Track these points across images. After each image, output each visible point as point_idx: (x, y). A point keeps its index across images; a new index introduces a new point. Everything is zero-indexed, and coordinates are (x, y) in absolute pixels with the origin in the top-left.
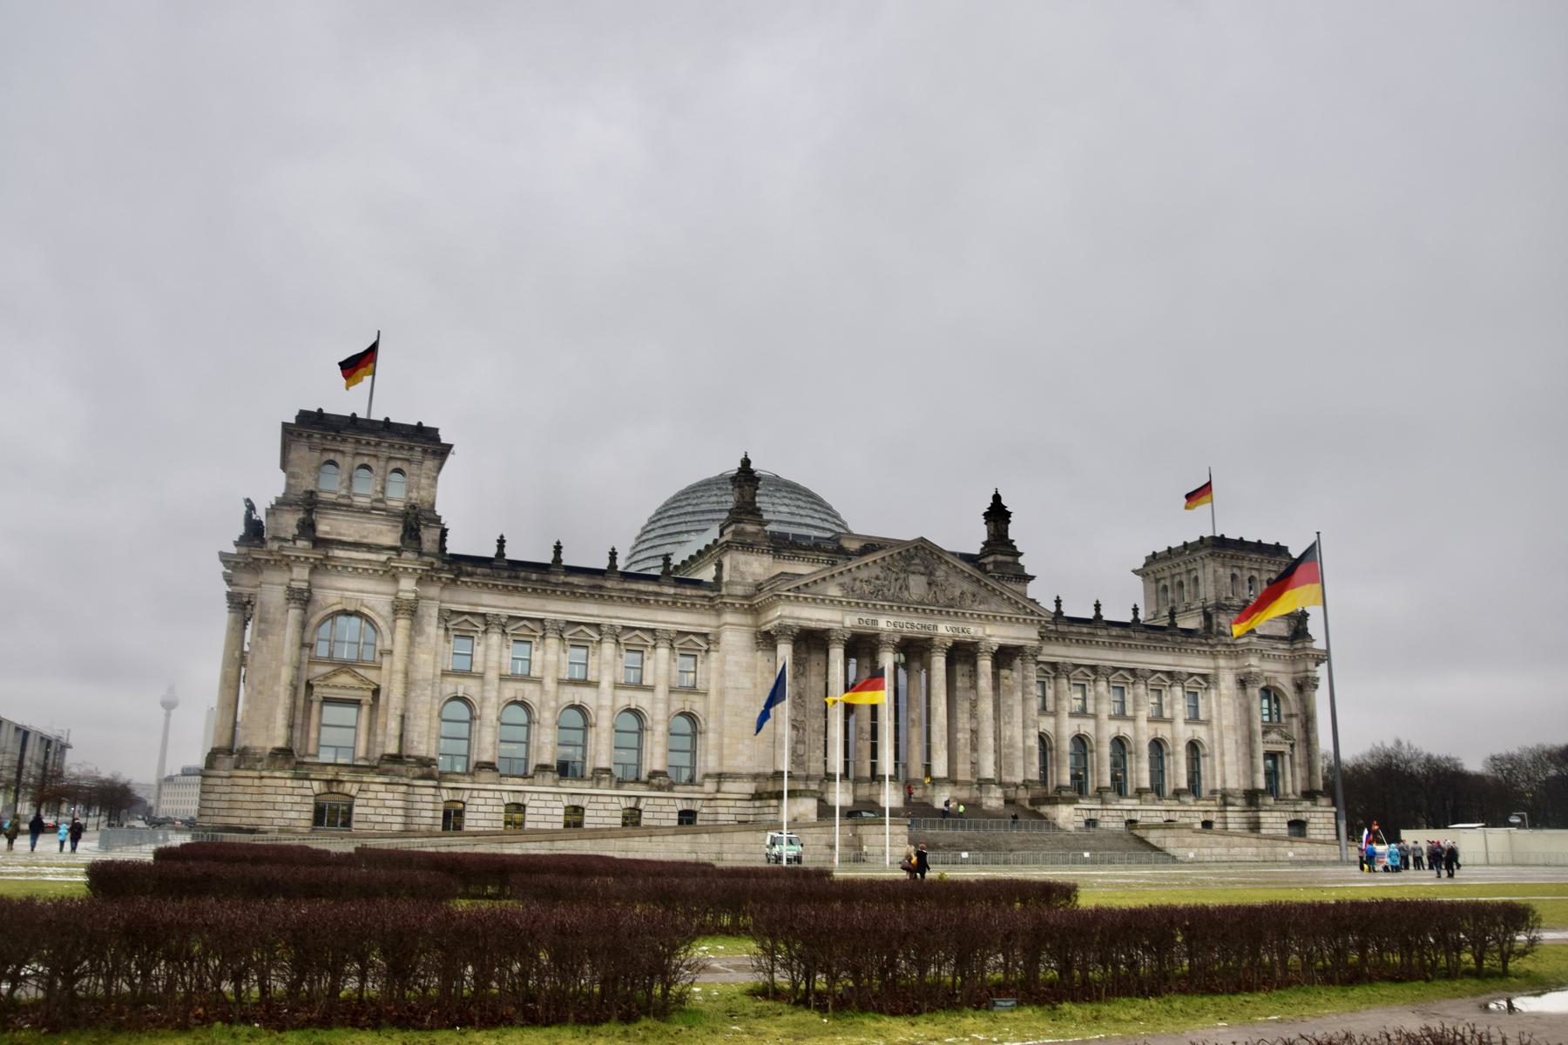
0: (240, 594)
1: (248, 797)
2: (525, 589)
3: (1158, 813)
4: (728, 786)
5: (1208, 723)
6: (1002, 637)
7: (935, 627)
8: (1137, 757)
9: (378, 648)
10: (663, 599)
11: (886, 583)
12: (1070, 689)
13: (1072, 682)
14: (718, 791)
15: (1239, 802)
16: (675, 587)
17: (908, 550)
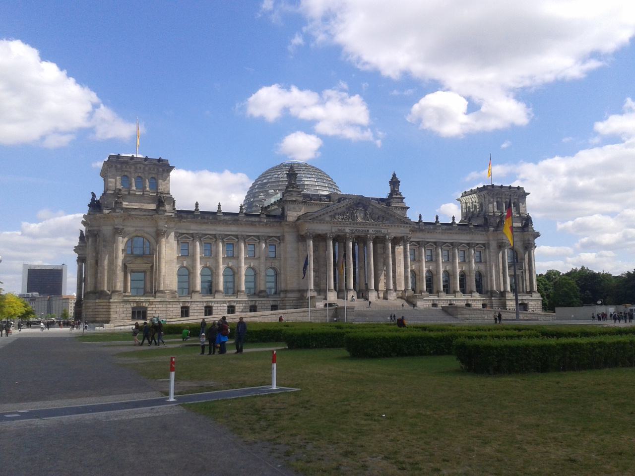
0: (94, 230)
1: (105, 310)
2: (207, 223)
4: (289, 295)
7: (368, 231)
8: (455, 278)
9: (151, 249)
14: (286, 297)
16: (266, 218)
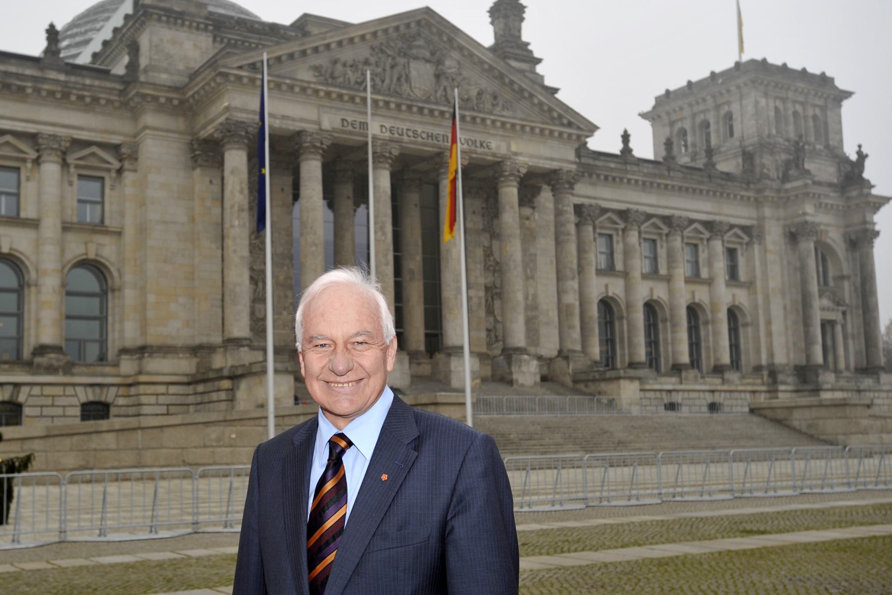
3: (702, 394)
5: (750, 285)
6: (531, 156)
8: (674, 325)
10: (46, 87)
11: (379, 70)
12: (595, 240)
13: (598, 231)
14: (140, 373)
15: (790, 379)
16: (67, 73)
17: (408, 26)
